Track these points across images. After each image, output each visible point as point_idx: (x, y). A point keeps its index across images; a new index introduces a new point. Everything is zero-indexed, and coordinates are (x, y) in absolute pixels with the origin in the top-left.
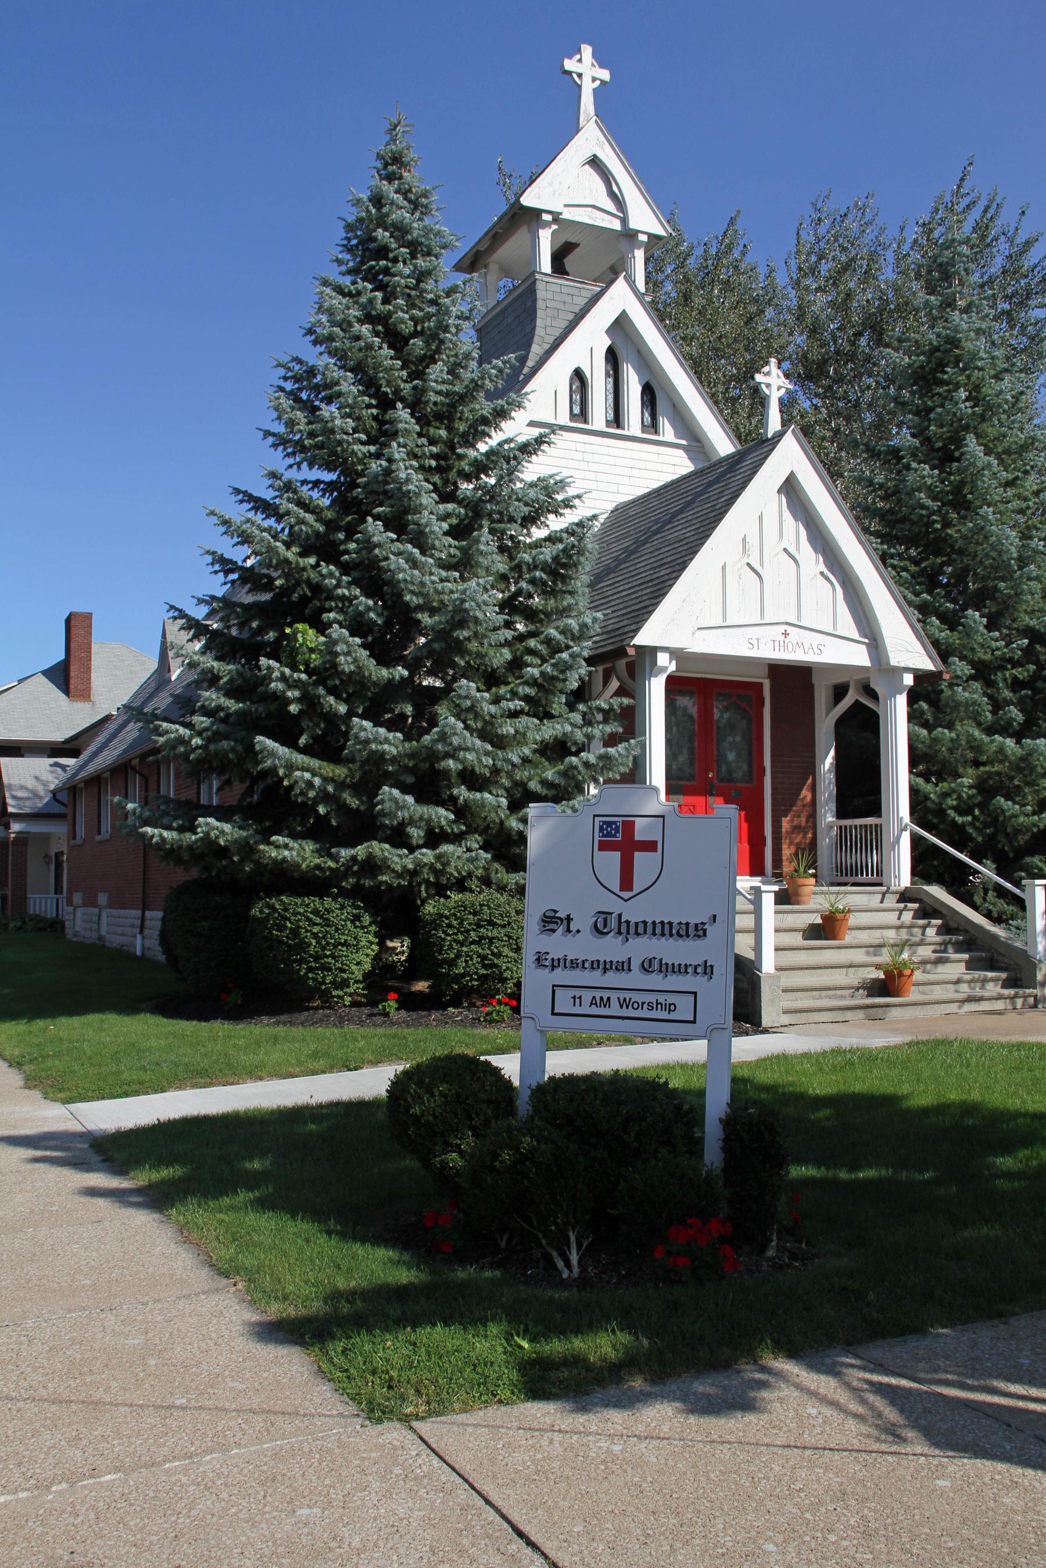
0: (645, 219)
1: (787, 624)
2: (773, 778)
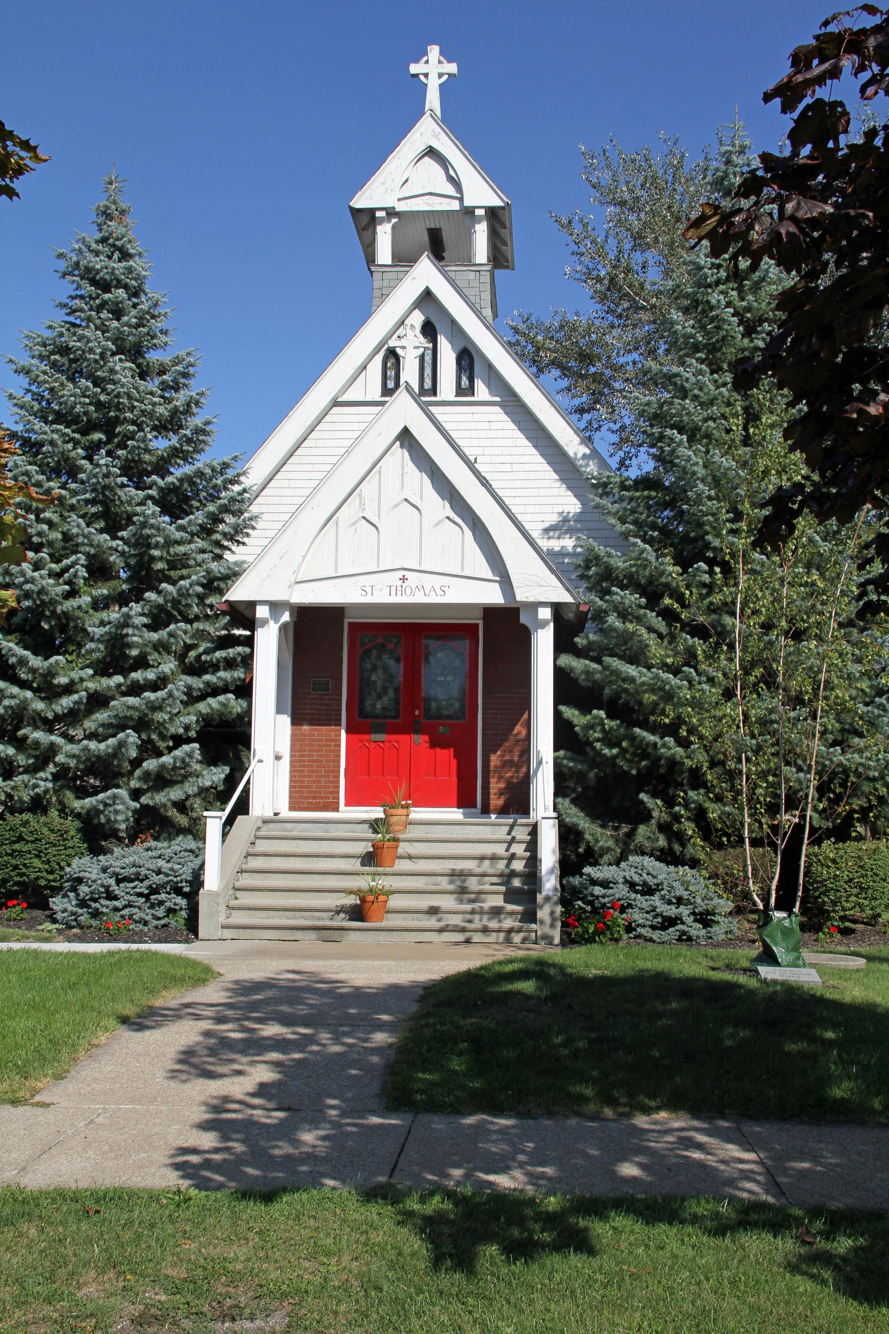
0: (481, 194)
1: (404, 569)
2: (483, 714)
